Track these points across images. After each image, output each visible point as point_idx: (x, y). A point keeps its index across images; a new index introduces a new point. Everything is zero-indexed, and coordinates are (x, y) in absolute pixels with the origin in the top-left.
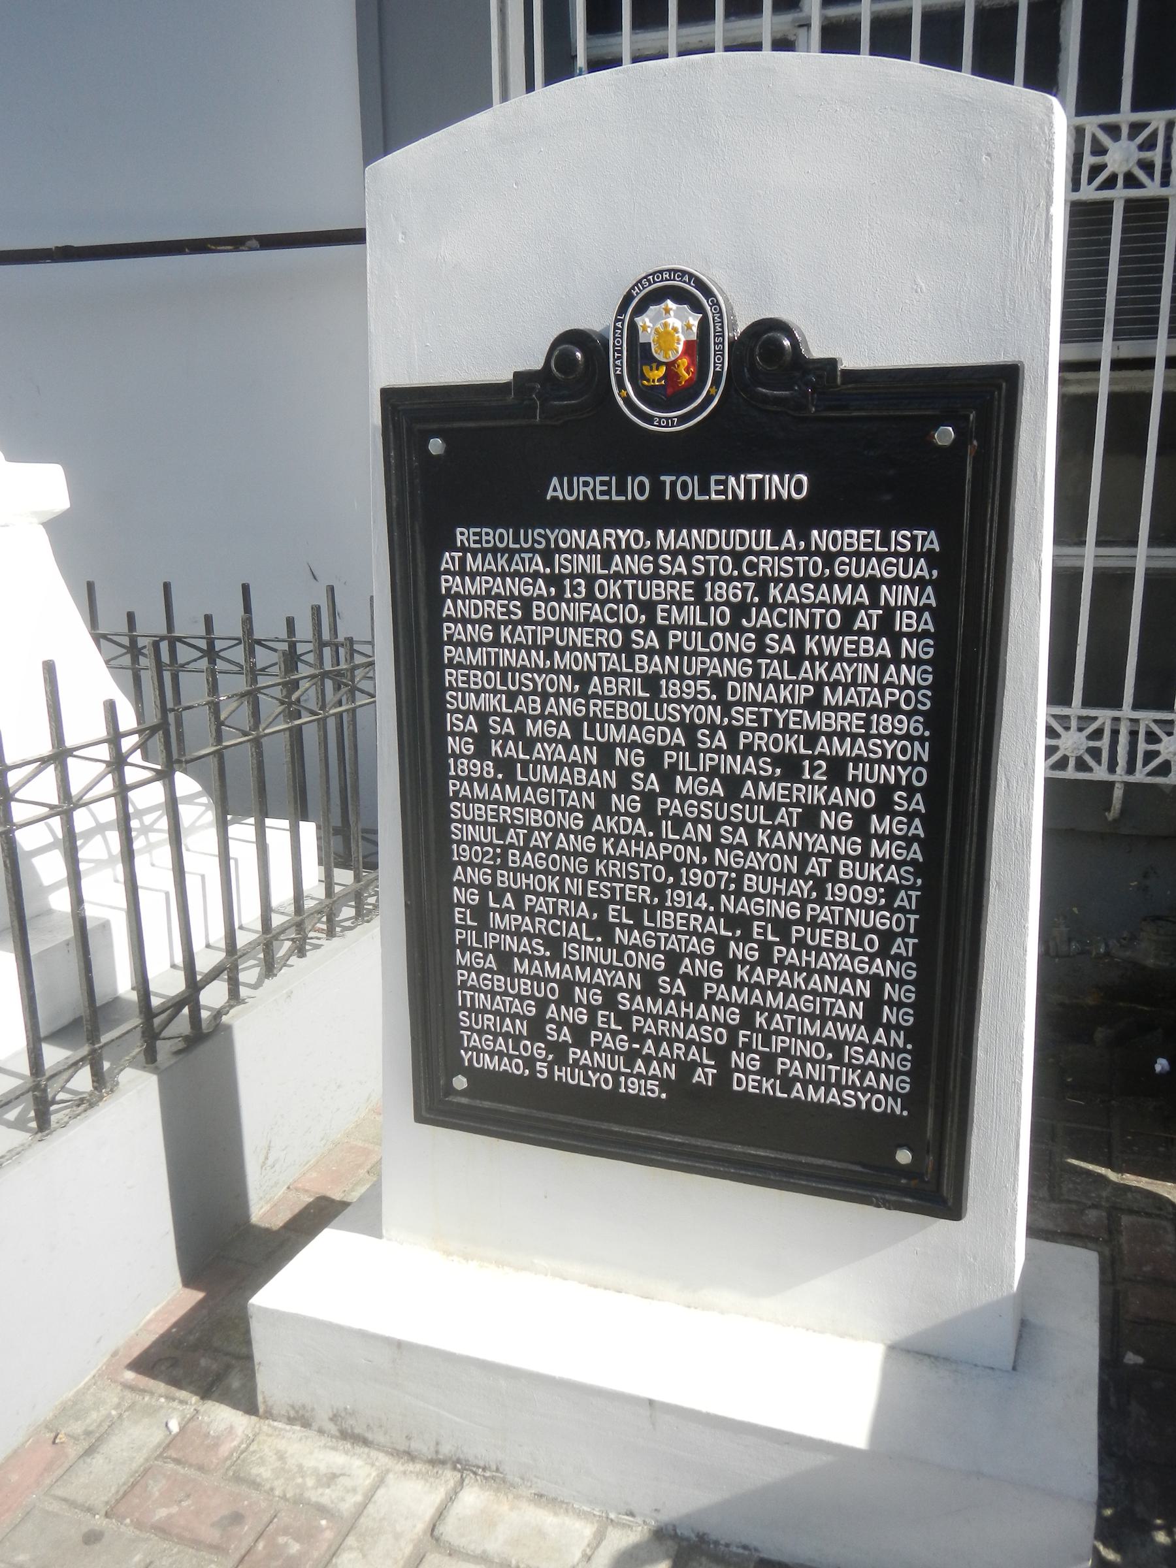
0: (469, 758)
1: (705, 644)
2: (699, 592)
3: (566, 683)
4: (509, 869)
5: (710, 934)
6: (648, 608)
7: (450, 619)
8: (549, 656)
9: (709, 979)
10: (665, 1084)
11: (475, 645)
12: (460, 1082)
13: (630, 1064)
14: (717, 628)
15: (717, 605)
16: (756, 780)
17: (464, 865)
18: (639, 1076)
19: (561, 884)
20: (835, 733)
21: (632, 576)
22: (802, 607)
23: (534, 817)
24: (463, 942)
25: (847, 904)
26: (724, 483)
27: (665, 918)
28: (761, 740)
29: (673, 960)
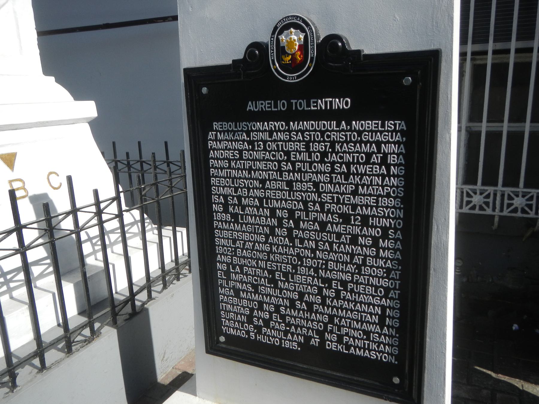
0: (221, 213)
1: (310, 168)
2: (307, 147)
3: (256, 184)
4: (237, 257)
5: (315, 285)
6: (287, 153)
7: (212, 158)
8: (250, 173)
9: (316, 303)
10: (299, 344)
11: (222, 169)
12: (222, 339)
13: (286, 335)
15: (315, 152)
17: (221, 255)
18: (289, 340)
19: (257, 263)
20: (364, 205)
21: (281, 141)
22: (349, 153)
24: (221, 284)
25: (370, 275)
26: (317, 102)
27: (297, 278)
28: (334, 207)
29: (301, 295)
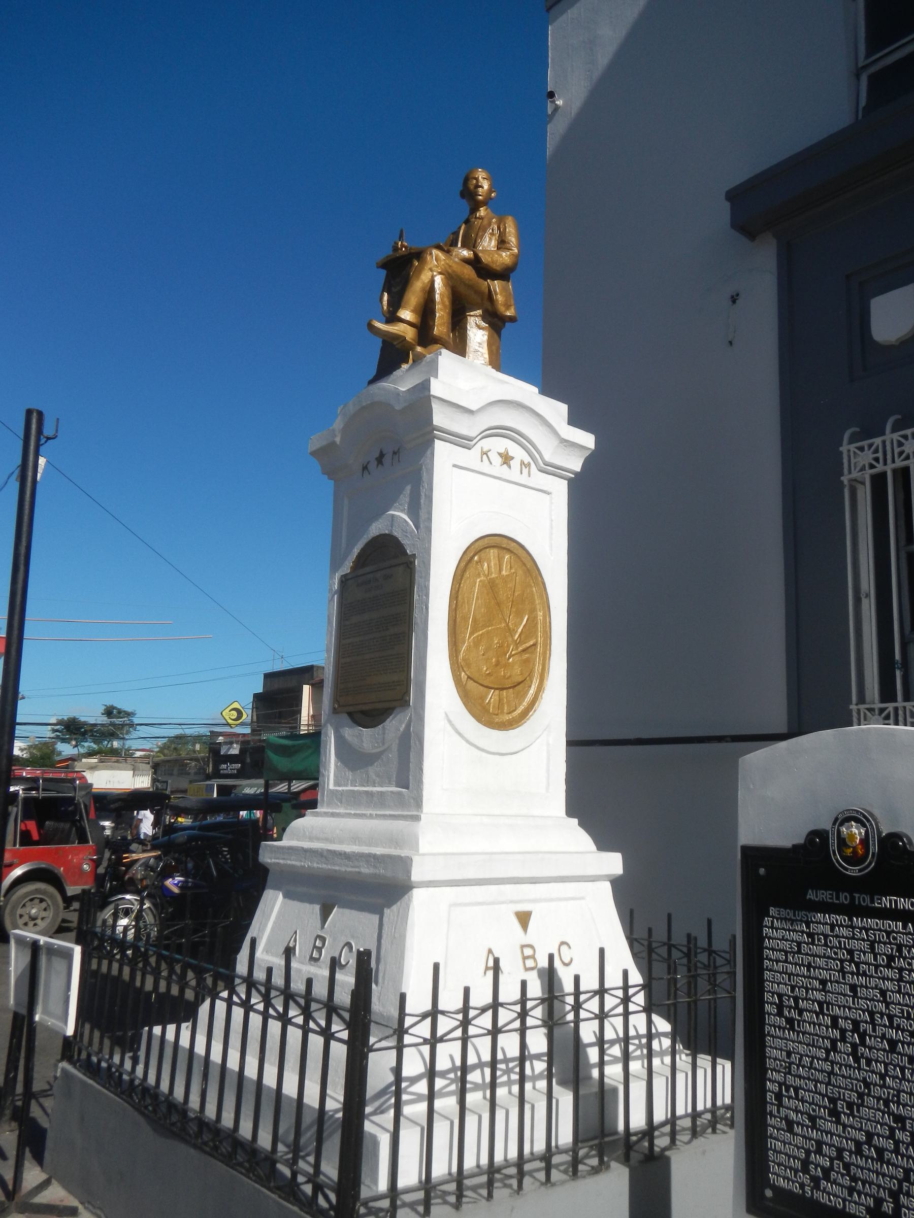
0: (774, 1015)
1: (876, 972)
3: (816, 984)
4: (792, 1075)
5: (886, 1124)
6: (851, 952)
8: (809, 970)
10: (868, 1210)
11: (777, 961)
12: (769, 1193)
13: (851, 1195)
14: (881, 966)
15: (880, 955)
16: (903, 1043)
18: (855, 1203)
19: (816, 1086)
21: (843, 937)
23: (802, 1049)
24: (771, 1112)
26: (881, 900)
27: (864, 1111)
29: (870, 1135)
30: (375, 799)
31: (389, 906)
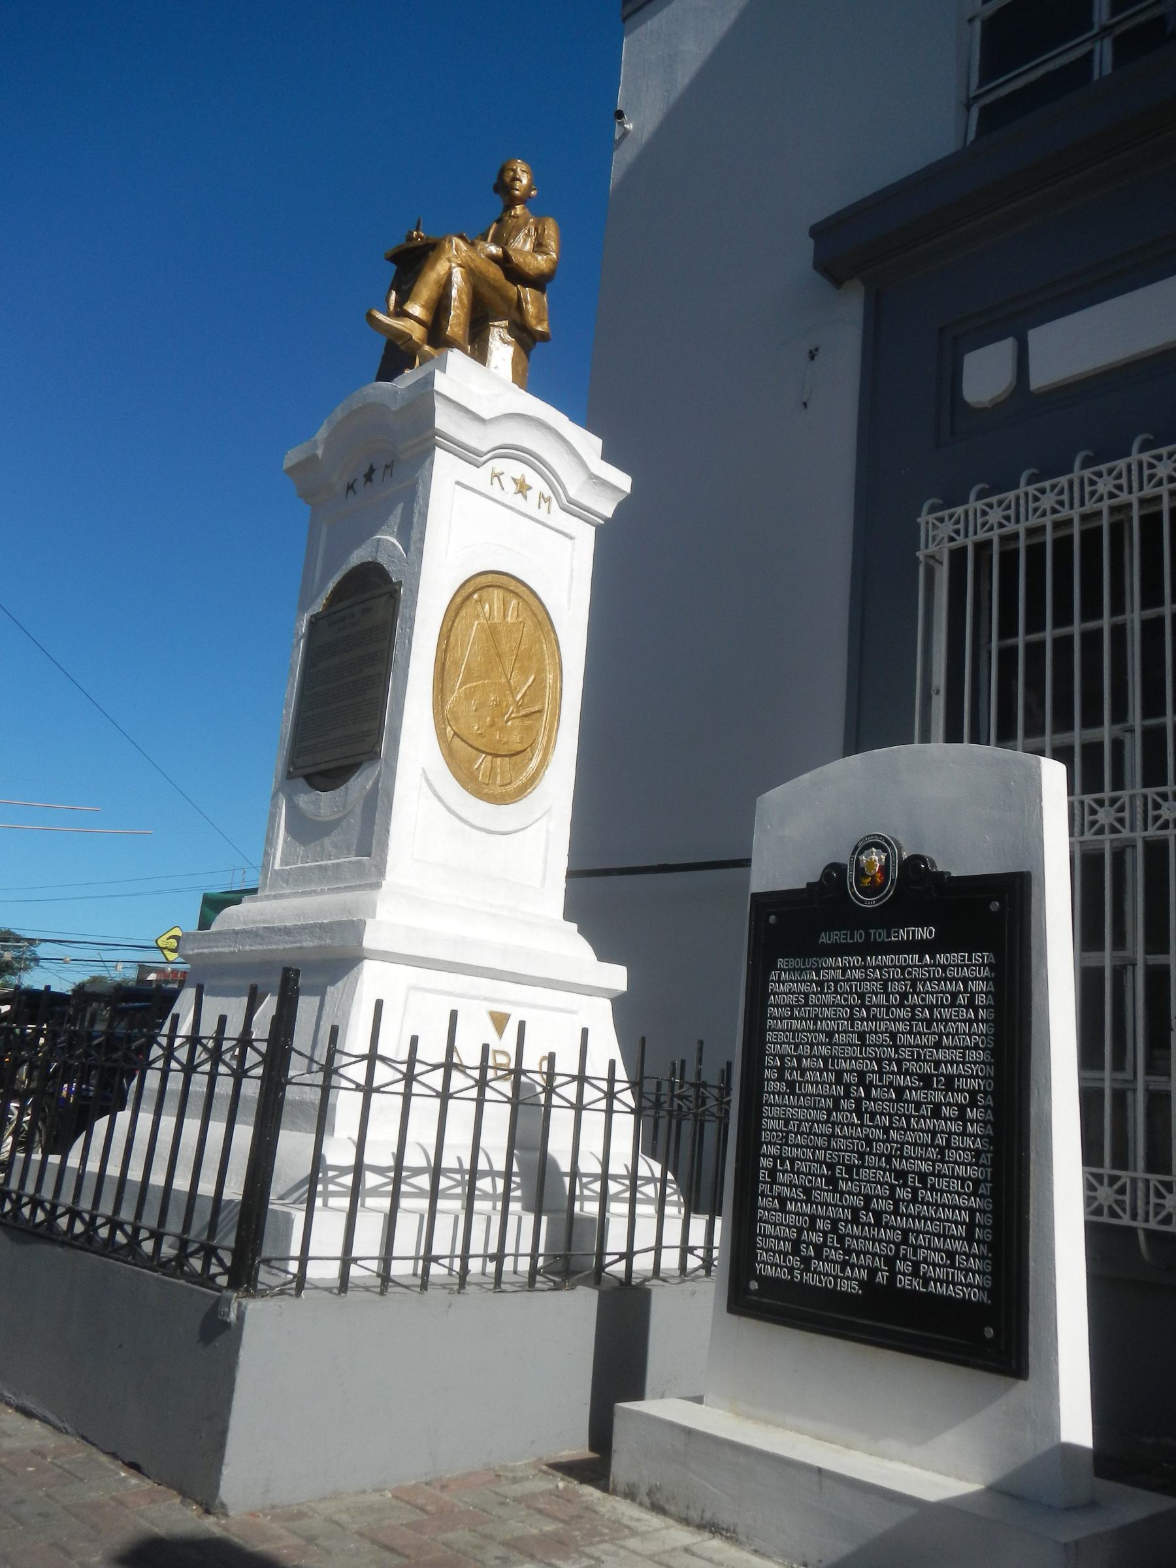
2: (885, 987)
3: (823, 1037)
5: (887, 1183)
6: (862, 996)
7: (771, 1005)
8: (815, 1024)
9: (886, 1212)
10: (861, 1284)
11: (781, 1019)
12: (754, 1285)
14: (893, 1006)
15: (893, 993)
16: (910, 1089)
17: (767, 1144)
18: (848, 1278)
19: (814, 1154)
20: (948, 1061)
21: (855, 980)
22: (932, 993)
23: (801, 1114)
24: (763, 1191)
25: (955, 1162)
28: (913, 1067)
29: (868, 1199)
30: (330, 873)
31: (333, 983)
